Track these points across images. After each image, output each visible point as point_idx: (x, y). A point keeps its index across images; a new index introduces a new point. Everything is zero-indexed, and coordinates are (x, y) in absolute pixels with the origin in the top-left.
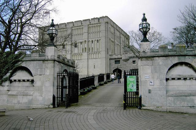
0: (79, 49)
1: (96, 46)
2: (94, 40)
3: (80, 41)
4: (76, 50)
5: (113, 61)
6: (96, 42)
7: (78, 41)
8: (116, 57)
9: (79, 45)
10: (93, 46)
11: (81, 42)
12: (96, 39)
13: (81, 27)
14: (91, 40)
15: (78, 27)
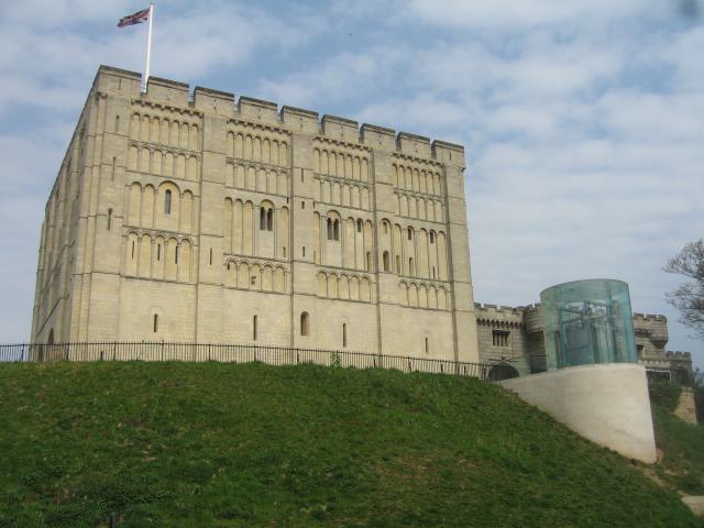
0: (350, 248)
1: (423, 256)
2: (417, 226)
3: (357, 214)
4: (333, 255)
5: (488, 330)
6: (422, 238)
7: (345, 213)
8: (500, 317)
9: (348, 229)
10: (410, 252)
11: (360, 221)
12: (428, 227)
13: (356, 152)
14: (404, 224)
15: (342, 149)
